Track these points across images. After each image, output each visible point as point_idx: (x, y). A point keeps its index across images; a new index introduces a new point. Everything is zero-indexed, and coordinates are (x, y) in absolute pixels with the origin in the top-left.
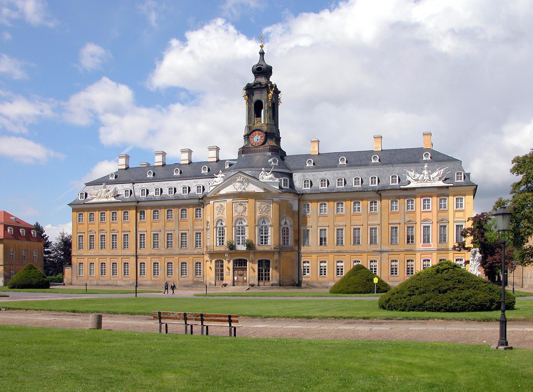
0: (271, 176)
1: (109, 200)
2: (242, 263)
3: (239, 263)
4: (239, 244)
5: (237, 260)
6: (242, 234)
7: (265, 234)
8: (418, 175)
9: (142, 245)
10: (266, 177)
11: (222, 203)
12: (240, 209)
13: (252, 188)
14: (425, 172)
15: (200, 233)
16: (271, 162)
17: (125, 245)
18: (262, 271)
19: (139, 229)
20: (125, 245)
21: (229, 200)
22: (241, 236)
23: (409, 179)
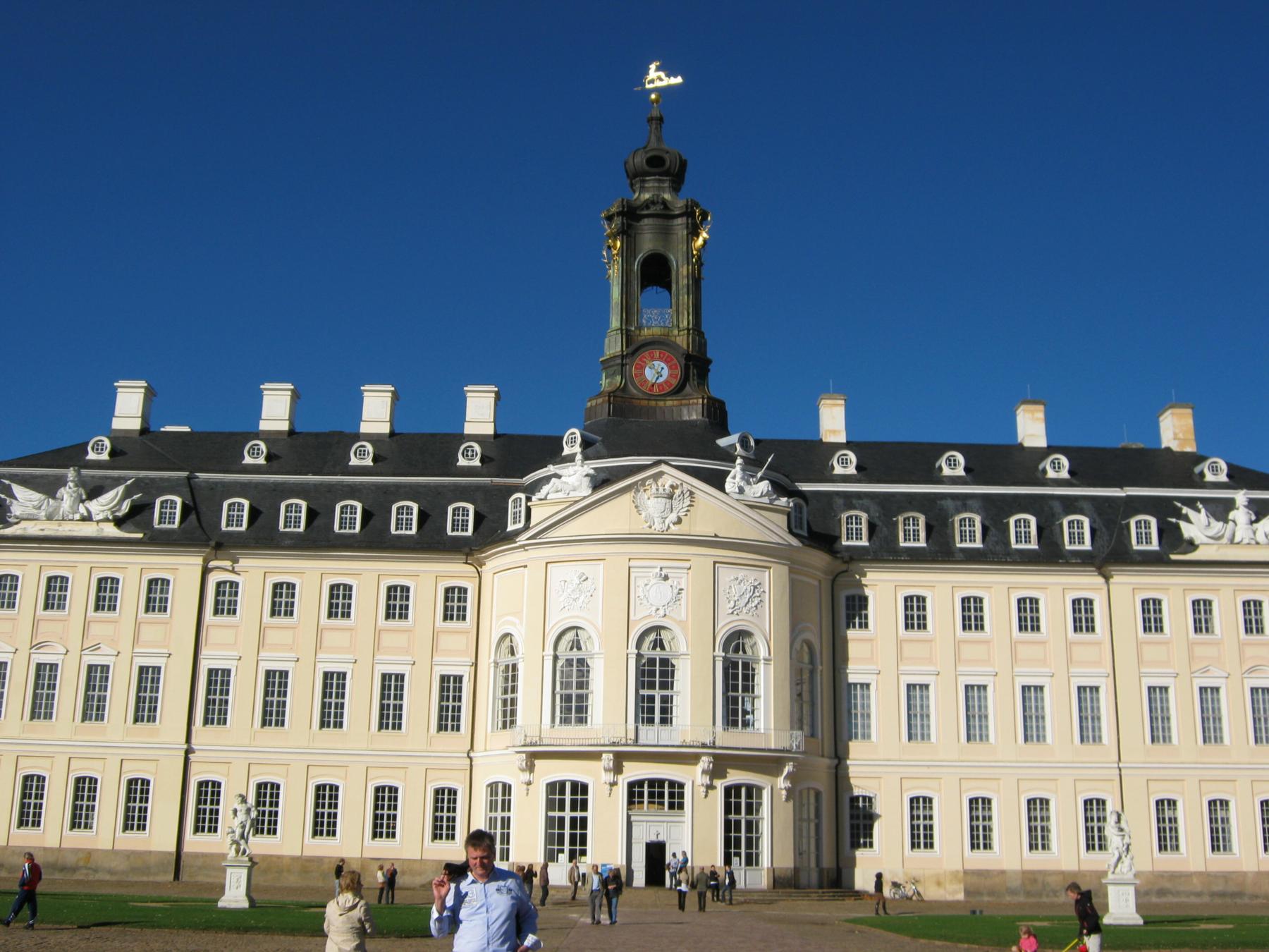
0: (764, 486)
1: (88, 530)
2: (661, 795)
3: (651, 795)
4: (651, 721)
5: (640, 783)
6: (664, 686)
7: (746, 689)
8: (1217, 526)
9: (216, 713)
10: (746, 487)
14: (1240, 515)
15: (459, 679)
16: (733, 446)
17: (145, 710)
18: (738, 830)
19: (205, 652)
20: (145, 710)
22: (657, 693)
23: (1187, 530)
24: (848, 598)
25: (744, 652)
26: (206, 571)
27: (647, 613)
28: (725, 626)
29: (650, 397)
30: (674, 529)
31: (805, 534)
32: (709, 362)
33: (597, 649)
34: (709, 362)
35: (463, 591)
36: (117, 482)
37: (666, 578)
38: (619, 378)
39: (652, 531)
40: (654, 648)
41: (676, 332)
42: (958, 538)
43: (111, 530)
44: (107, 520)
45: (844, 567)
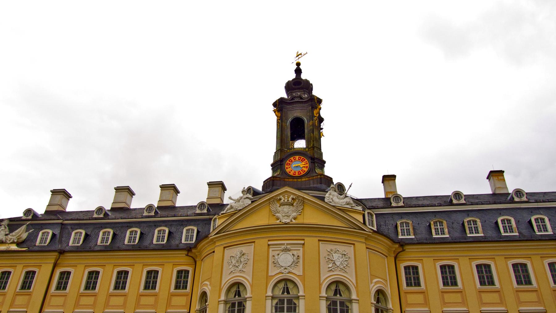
11: (244, 249)
12: (286, 259)
13: (312, 217)
21: (262, 242)
24: (405, 268)
25: (341, 295)
26: (55, 266)
27: (278, 271)
28: (327, 278)
29: (293, 177)
30: (294, 221)
31: (375, 229)
32: (324, 162)
33: (248, 295)
34: (324, 162)
35: (187, 272)
36: (24, 224)
37: (289, 250)
38: (279, 171)
39: (281, 223)
40: (283, 293)
41: (307, 149)
42: (468, 231)
43: (14, 247)
44: (13, 243)
45: (401, 249)
